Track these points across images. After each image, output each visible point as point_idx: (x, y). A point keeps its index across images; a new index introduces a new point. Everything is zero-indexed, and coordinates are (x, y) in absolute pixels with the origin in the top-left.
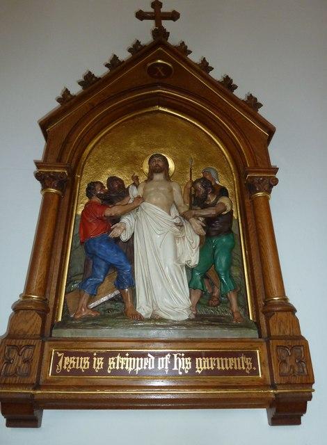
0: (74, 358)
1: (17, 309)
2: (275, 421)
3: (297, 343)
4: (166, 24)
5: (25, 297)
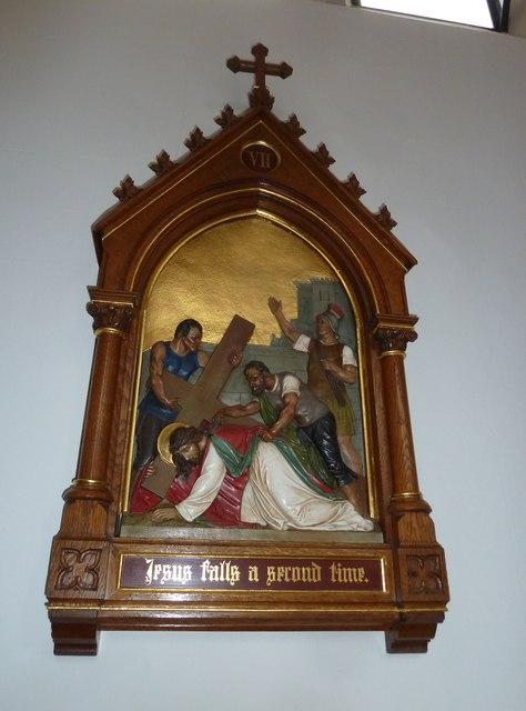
0: (168, 567)
1: (71, 497)
2: (395, 647)
3: (431, 552)
4: (272, 82)
5: (80, 483)
